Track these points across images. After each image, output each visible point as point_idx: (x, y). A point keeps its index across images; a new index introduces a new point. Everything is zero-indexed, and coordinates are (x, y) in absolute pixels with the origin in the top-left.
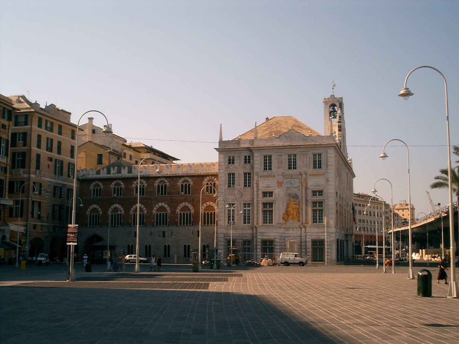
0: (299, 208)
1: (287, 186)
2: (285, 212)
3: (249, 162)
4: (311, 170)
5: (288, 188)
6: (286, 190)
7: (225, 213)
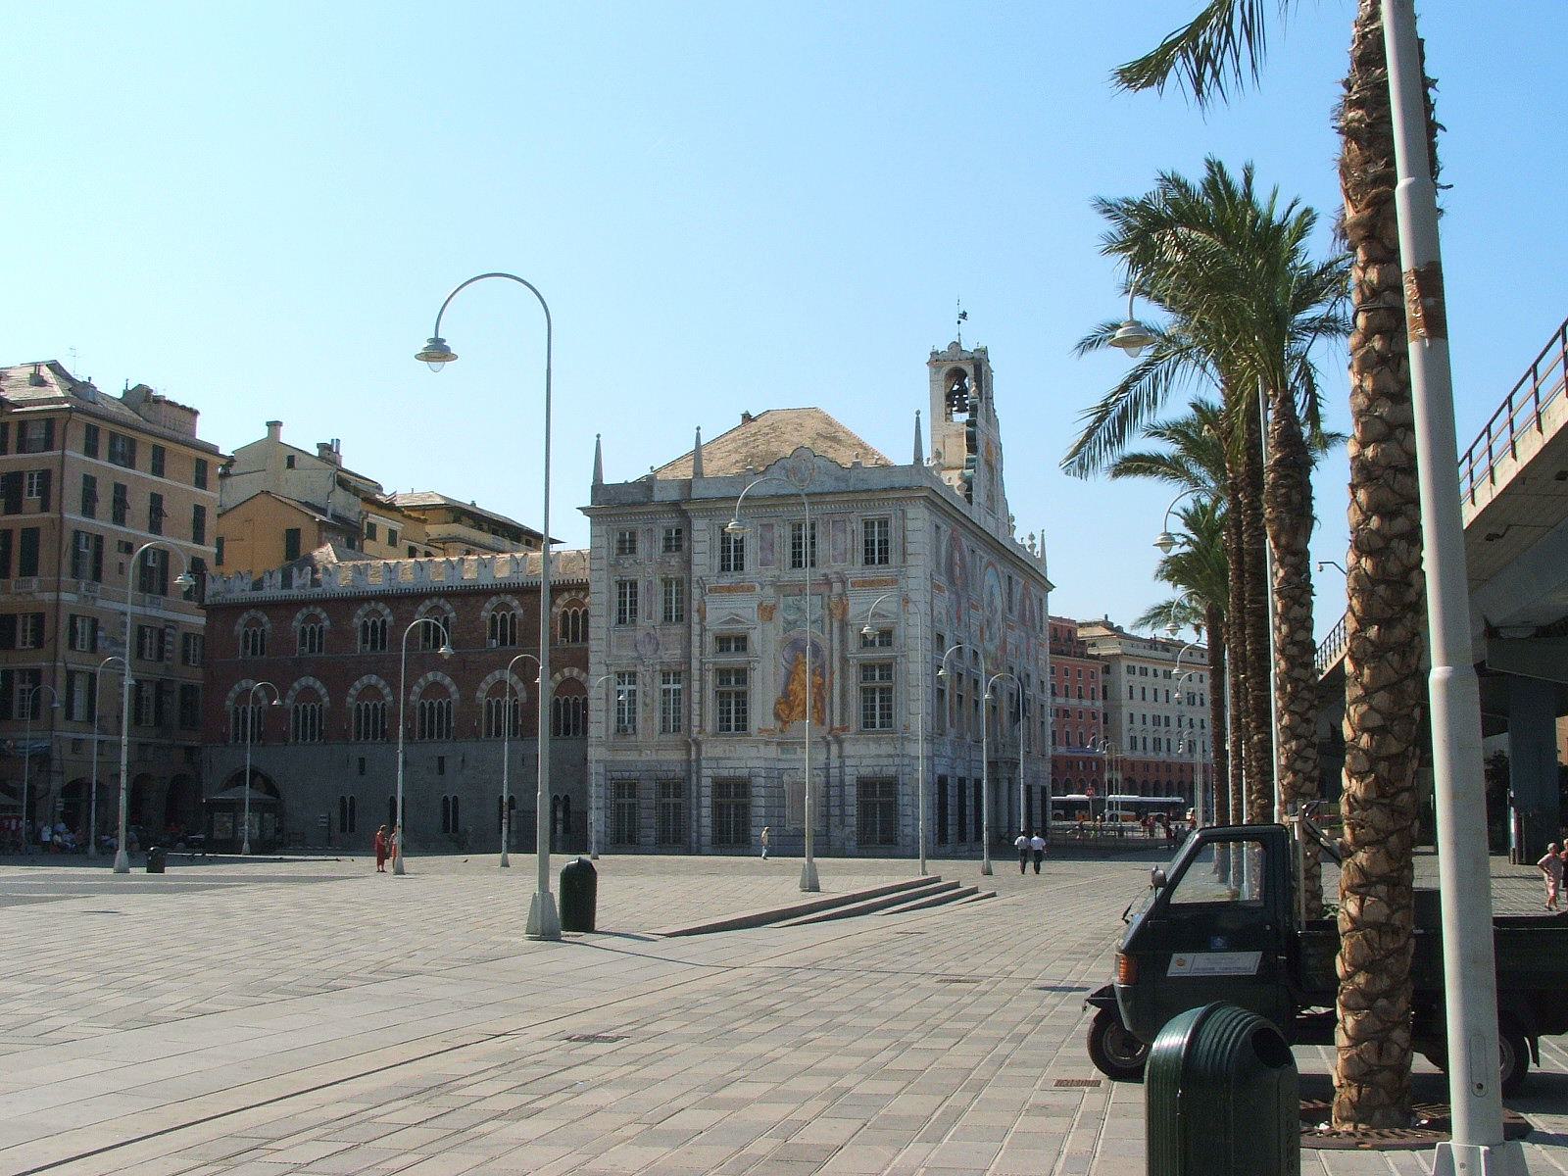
0: (823, 683)
3: (679, 548)
4: (856, 570)
5: (790, 625)
7: (607, 700)
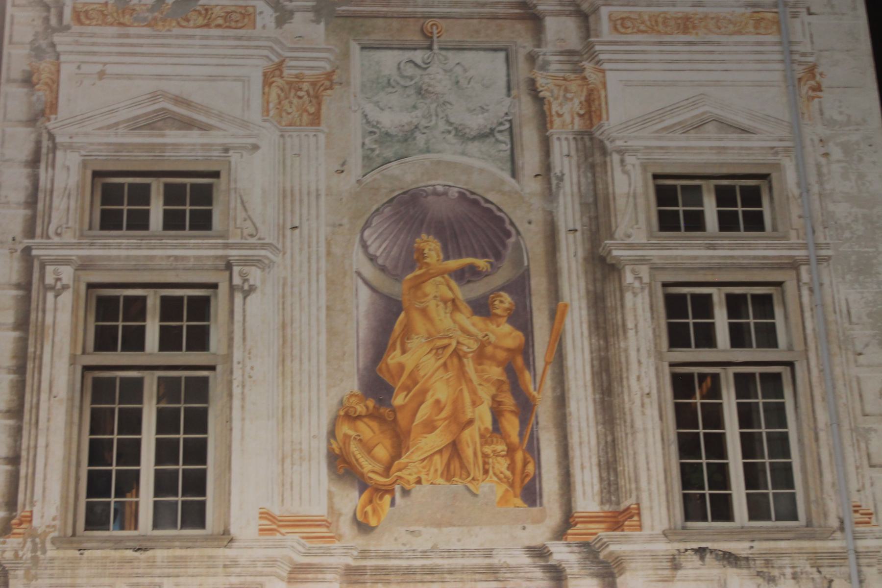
0: (526, 350)
1: (374, 114)
2: (353, 385)
5: (386, 145)
6: (370, 162)
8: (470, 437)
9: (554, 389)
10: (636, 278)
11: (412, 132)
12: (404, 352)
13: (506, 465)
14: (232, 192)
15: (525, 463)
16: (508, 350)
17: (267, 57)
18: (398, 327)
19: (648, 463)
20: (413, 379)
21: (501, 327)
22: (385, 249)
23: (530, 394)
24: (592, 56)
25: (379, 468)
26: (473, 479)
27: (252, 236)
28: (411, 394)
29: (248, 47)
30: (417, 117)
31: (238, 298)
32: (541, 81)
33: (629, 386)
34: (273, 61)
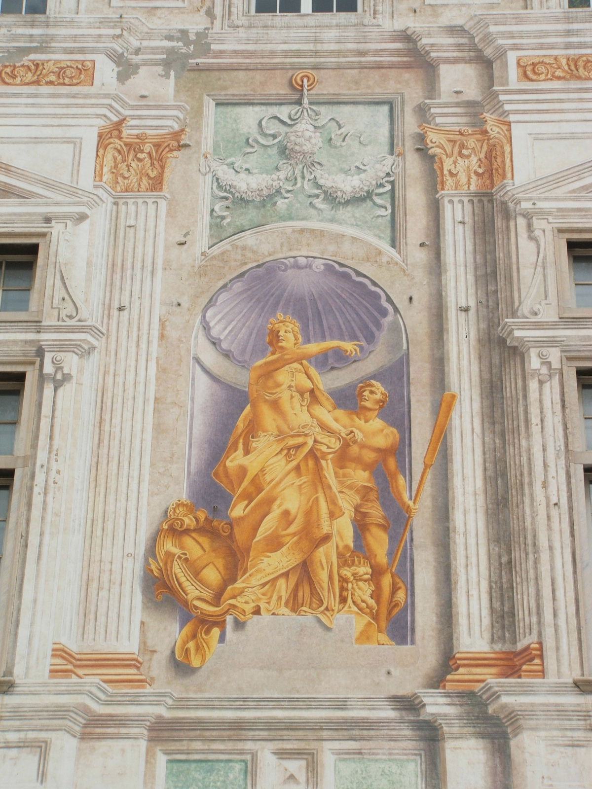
0: (400, 451)
1: (226, 175)
2: (182, 492)
8: (326, 555)
9: (434, 498)
10: (543, 363)
11: (270, 196)
12: (247, 452)
13: (369, 592)
14: (51, 268)
15: (394, 589)
16: (378, 450)
17: (105, 116)
18: (241, 424)
19: (554, 591)
20: (257, 485)
21: (371, 421)
22: (230, 332)
23: (404, 504)
24: (497, 107)
25: (207, 595)
26: (327, 609)
27: (70, 317)
28: (253, 504)
29: (83, 106)
30: (279, 179)
31: (48, 390)
32: (432, 137)
33: (532, 495)
34: (111, 120)
